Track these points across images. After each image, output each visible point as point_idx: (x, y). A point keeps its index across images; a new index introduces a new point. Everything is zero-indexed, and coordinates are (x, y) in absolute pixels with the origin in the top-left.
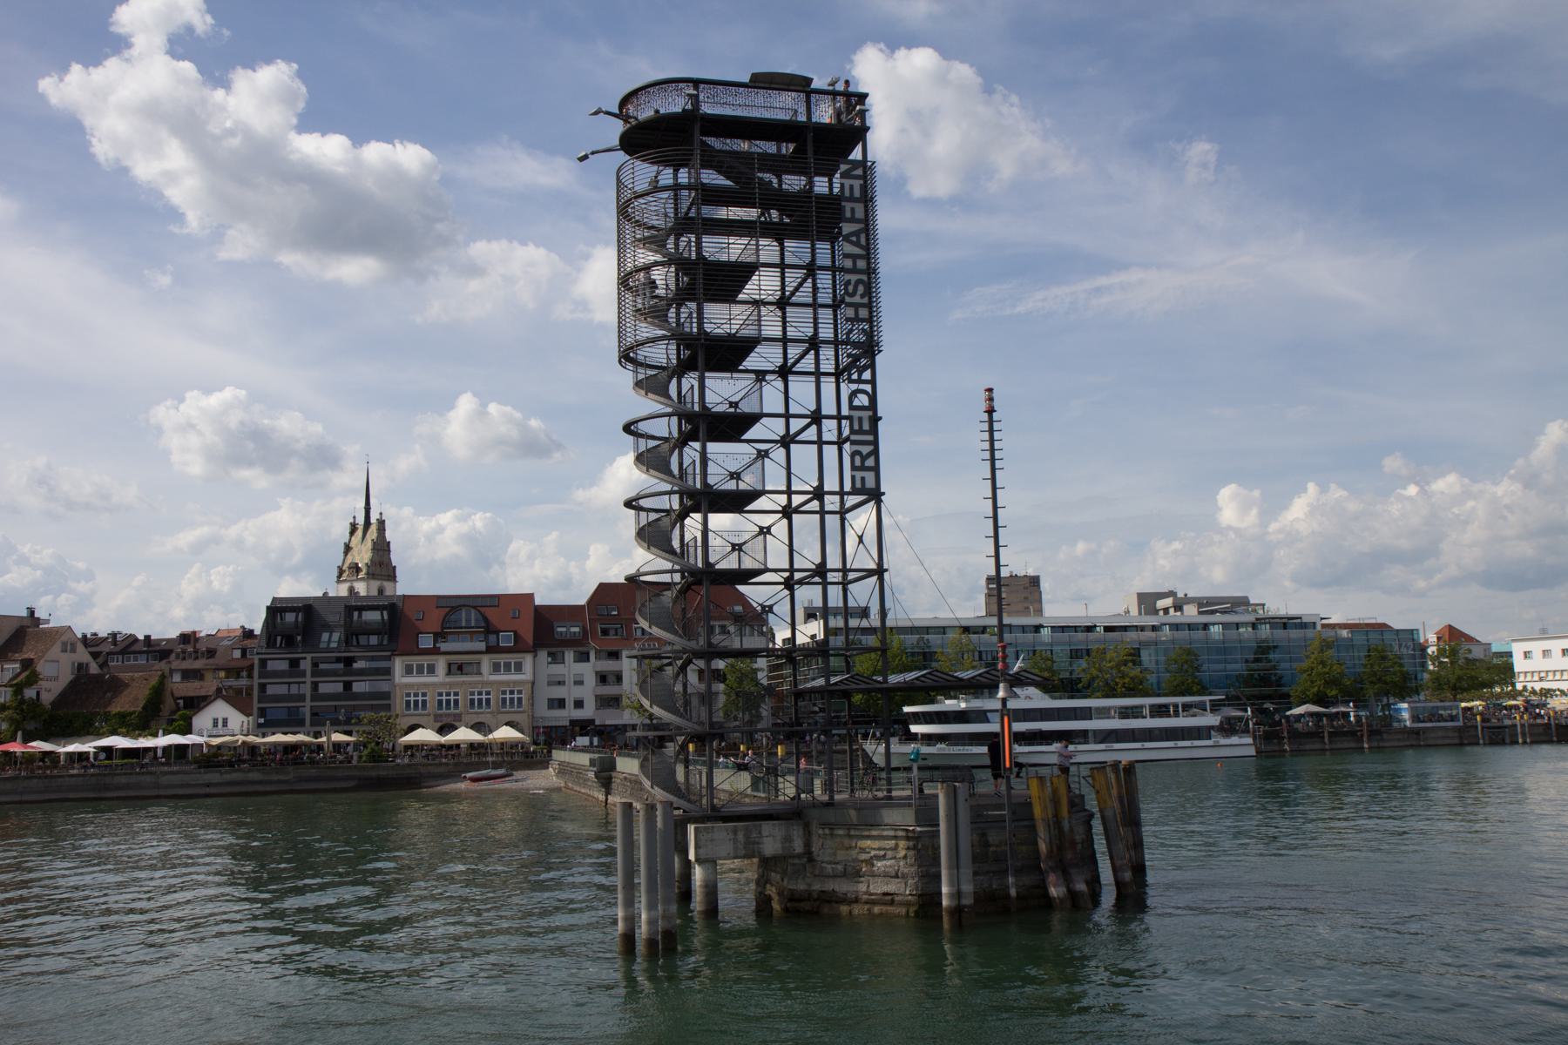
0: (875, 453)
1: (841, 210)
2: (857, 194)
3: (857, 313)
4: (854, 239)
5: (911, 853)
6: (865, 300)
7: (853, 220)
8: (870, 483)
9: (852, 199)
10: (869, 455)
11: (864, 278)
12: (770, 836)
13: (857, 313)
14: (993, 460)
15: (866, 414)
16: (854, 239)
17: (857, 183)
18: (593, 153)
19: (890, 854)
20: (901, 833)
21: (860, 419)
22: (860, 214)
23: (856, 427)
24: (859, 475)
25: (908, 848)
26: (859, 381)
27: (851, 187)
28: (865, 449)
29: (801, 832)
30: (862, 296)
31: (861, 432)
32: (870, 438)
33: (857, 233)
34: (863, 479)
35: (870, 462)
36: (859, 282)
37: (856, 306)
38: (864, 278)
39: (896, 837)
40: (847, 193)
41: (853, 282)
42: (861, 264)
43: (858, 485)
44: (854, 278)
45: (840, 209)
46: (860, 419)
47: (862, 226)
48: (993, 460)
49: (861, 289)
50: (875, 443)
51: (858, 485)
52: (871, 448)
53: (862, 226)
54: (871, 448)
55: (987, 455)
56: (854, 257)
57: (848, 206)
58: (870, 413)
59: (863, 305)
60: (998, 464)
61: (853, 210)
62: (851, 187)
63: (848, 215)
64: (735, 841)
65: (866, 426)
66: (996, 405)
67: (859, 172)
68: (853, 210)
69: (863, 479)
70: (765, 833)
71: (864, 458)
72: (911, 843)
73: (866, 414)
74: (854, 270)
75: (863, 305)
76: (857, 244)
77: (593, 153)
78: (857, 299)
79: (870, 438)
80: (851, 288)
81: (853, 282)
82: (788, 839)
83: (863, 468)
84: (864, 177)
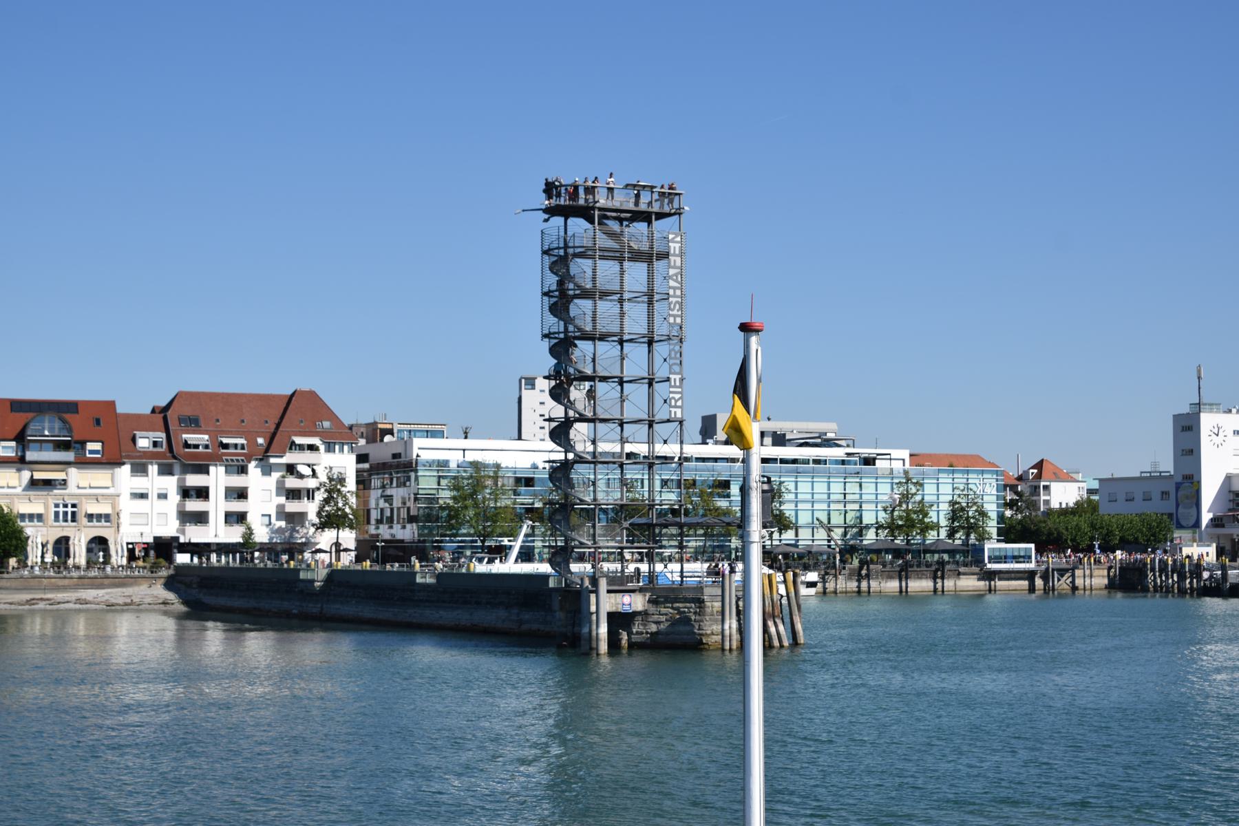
2: (677, 252)
7: (675, 267)
8: (679, 415)
9: (675, 255)
10: (679, 399)
15: (678, 377)
17: (678, 246)
18: (524, 211)
21: (675, 380)
23: (673, 384)
24: (673, 410)
26: (675, 358)
27: (675, 248)
28: (677, 396)
30: (678, 311)
31: (675, 386)
32: (680, 390)
33: (676, 275)
34: (675, 412)
35: (679, 403)
36: (677, 302)
37: (675, 316)
40: (672, 252)
43: (673, 416)
46: (675, 380)
49: (677, 307)
51: (673, 416)
52: (680, 395)
54: (680, 395)
56: (675, 288)
59: (678, 316)
61: (675, 261)
62: (675, 248)
65: (678, 384)
68: (675, 261)
69: (675, 412)
71: (676, 401)
73: (678, 377)
74: (675, 296)
76: (676, 281)
78: (675, 312)
79: (680, 390)
83: (676, 407)
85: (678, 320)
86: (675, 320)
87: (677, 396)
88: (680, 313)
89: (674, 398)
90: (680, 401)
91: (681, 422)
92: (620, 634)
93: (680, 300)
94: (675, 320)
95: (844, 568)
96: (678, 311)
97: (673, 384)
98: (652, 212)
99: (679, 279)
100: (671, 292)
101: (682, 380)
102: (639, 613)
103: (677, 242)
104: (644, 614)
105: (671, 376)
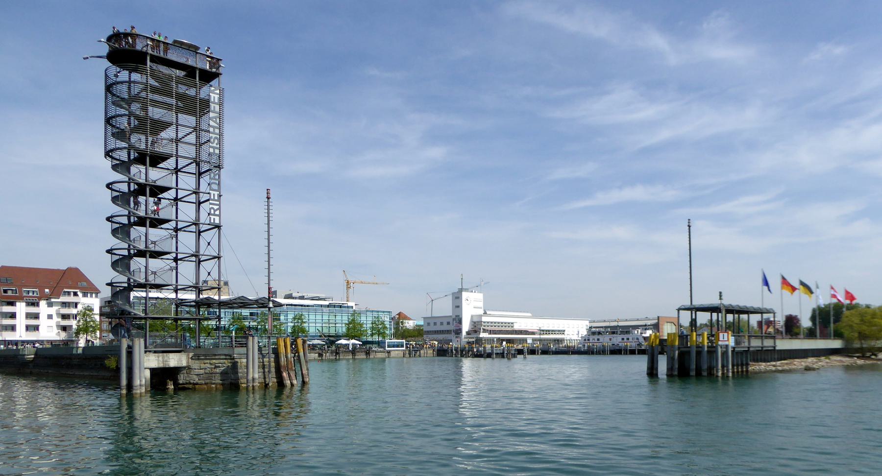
0: (219, 209)
1: (209, 106)
2: (216, 101)
7: (214, 112)
8: (217, 221)
9: (214, 103)
10: (217, 210)
14: (268, 217)
15: (216, 193)
20: (227, 357)
21: (214, 194)
24: (212, 217)
26: (215, 179)
28: (216, 207)
29: (185, 358)
32: (218, 203)
33: (215, 118)
34: (214, 219)
36: (216, 138)
37: (214, 148)
40: (212, 100)
43: (212, 221)
44: (214, 136)
45: (209, 106)
46: (214, 194)
48: (268, 217)
49: (216, 141)
50: (219, 205)
51: (212, 221)
55: (267, 215)
56: (214, 127)
57: (212, 105)
58: (218, 193)
59: (217, 148)
60: (271, 219)
63: (212, 109)
64: (158, 360)
65: (216, 198)
66: (271, 196)
69: (214, 219)
70: (170, 358)
71: (215, 211)
73: (216, 193)
74: (214, 133)
75: (217, 148)
76: (215, 122)
77: (91, 57)
78: (214, 145)
79: (218, 203)
82: (180, 360)
83: (214, 215)
85: (217, 151)
86: (214, 151)
87: (216, 207)
88: (218, 146)
90: (218, 211)
91: (218, 227)
92: (166, 384)
93: (218, 136)
94: (214, 151)
95: (329, 350)
98: (197, 68)
99: (218, 121)
100: (211, 130)
101: (220, 196)
102: (184, 368)
104: (188, 368)
105: (211, 192)
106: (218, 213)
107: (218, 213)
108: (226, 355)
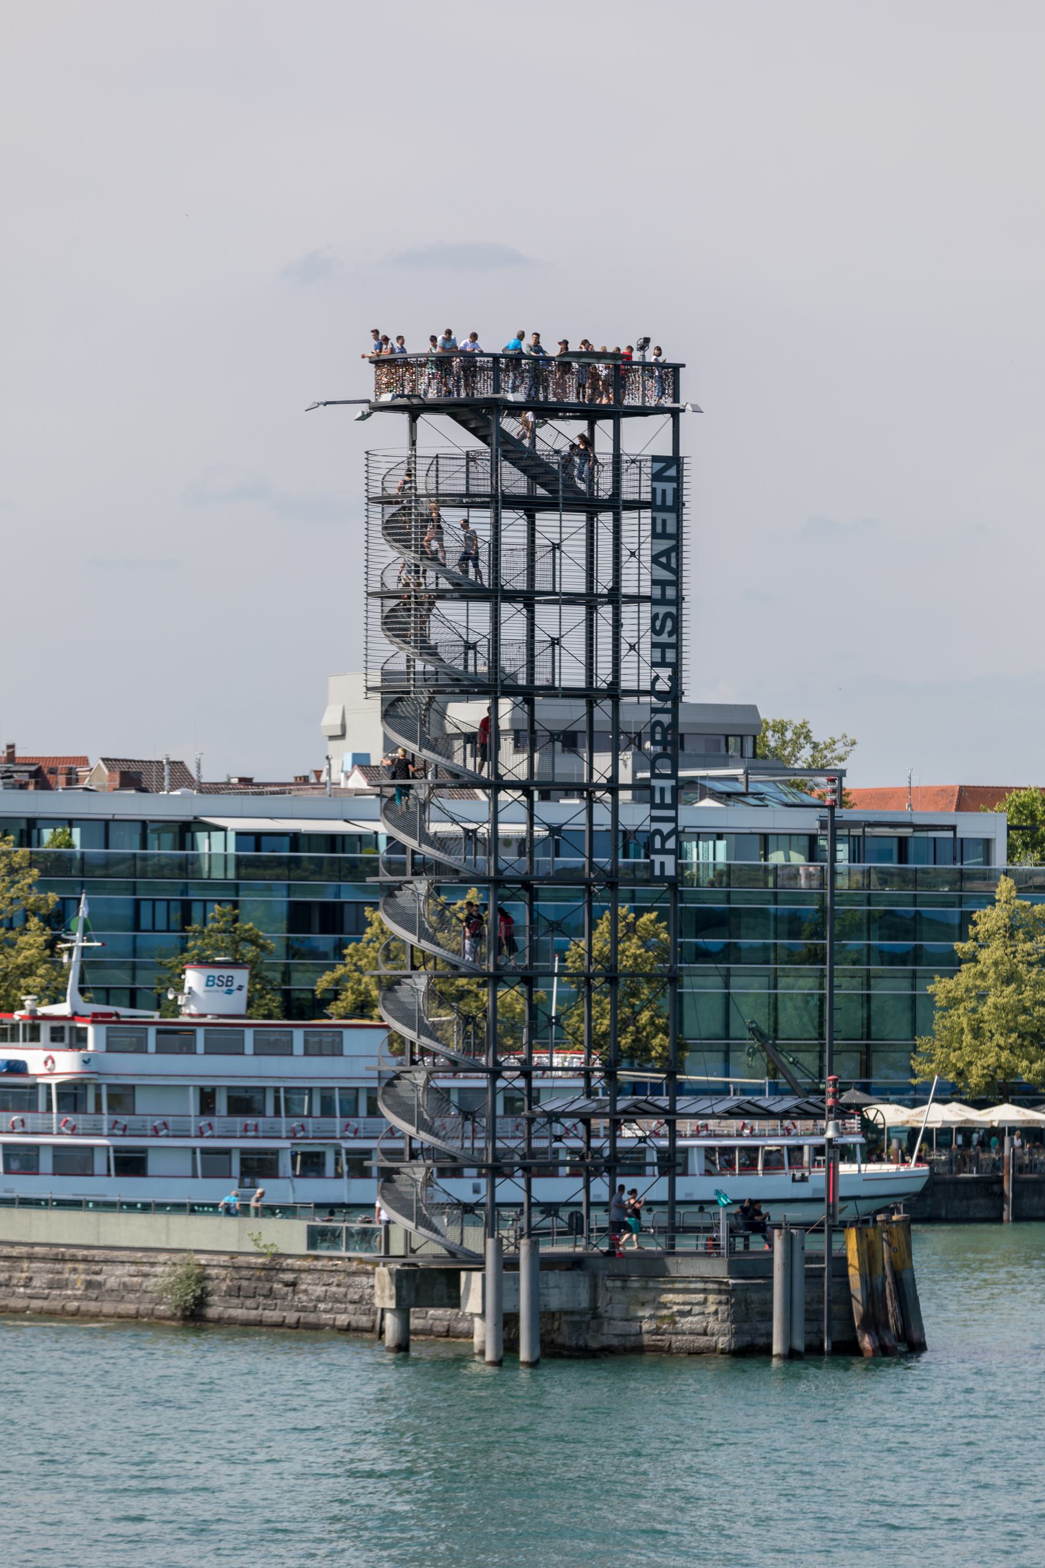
2: (669, 502)
3: (663, 656)
4: (663, 560)
5: (723, 1308)
6: (673, 640)
11: (673, 610)
12: (557, 1287)
13: (663, 656)
16: (663, 560)
17: (670, 487)
19: (697, 1309)
20: (711, 1286)
21: (662, 790)
22: (671, 529)
23: (658, 800)
24: (657, 859)
25: (720, 1303)
27: (664, 492)
28: (666, 827)
30: (670, 634)
31: (663, 806)
33: (666, 553)
34: (662, 864)
35: (671, 844)
36: (668, 615)
38: (673, 610)
39: (704, 1291)
41: (661, 617)
42: (671, 592)
43: (657, 872)
44: (662, 610)
46: (662, 790)
47: (673, 542)
49: (669, 624)
51: (657, 872)
52: (672, 826)
53: (673, 542)
54: (672, 826)
62: (664, 492)
65: (668, 800)
67: (672, 472)
69: (662, 864)
71: (664, 839)
72: (724, 1298)
76: (666, 567)
78: (664, 638)
80: (658, 623)
81: (661, 617)
83: (663, 851)
84: (678, 479)
87: (666, 827)
89: (658, 832)
90: (673, 839)
96: (670, 634)
97: (658, 800)
99: (674, 565)
103: (669, 479)
106: (673, 847)
107: (673, 847)
108: (705, 1280)
